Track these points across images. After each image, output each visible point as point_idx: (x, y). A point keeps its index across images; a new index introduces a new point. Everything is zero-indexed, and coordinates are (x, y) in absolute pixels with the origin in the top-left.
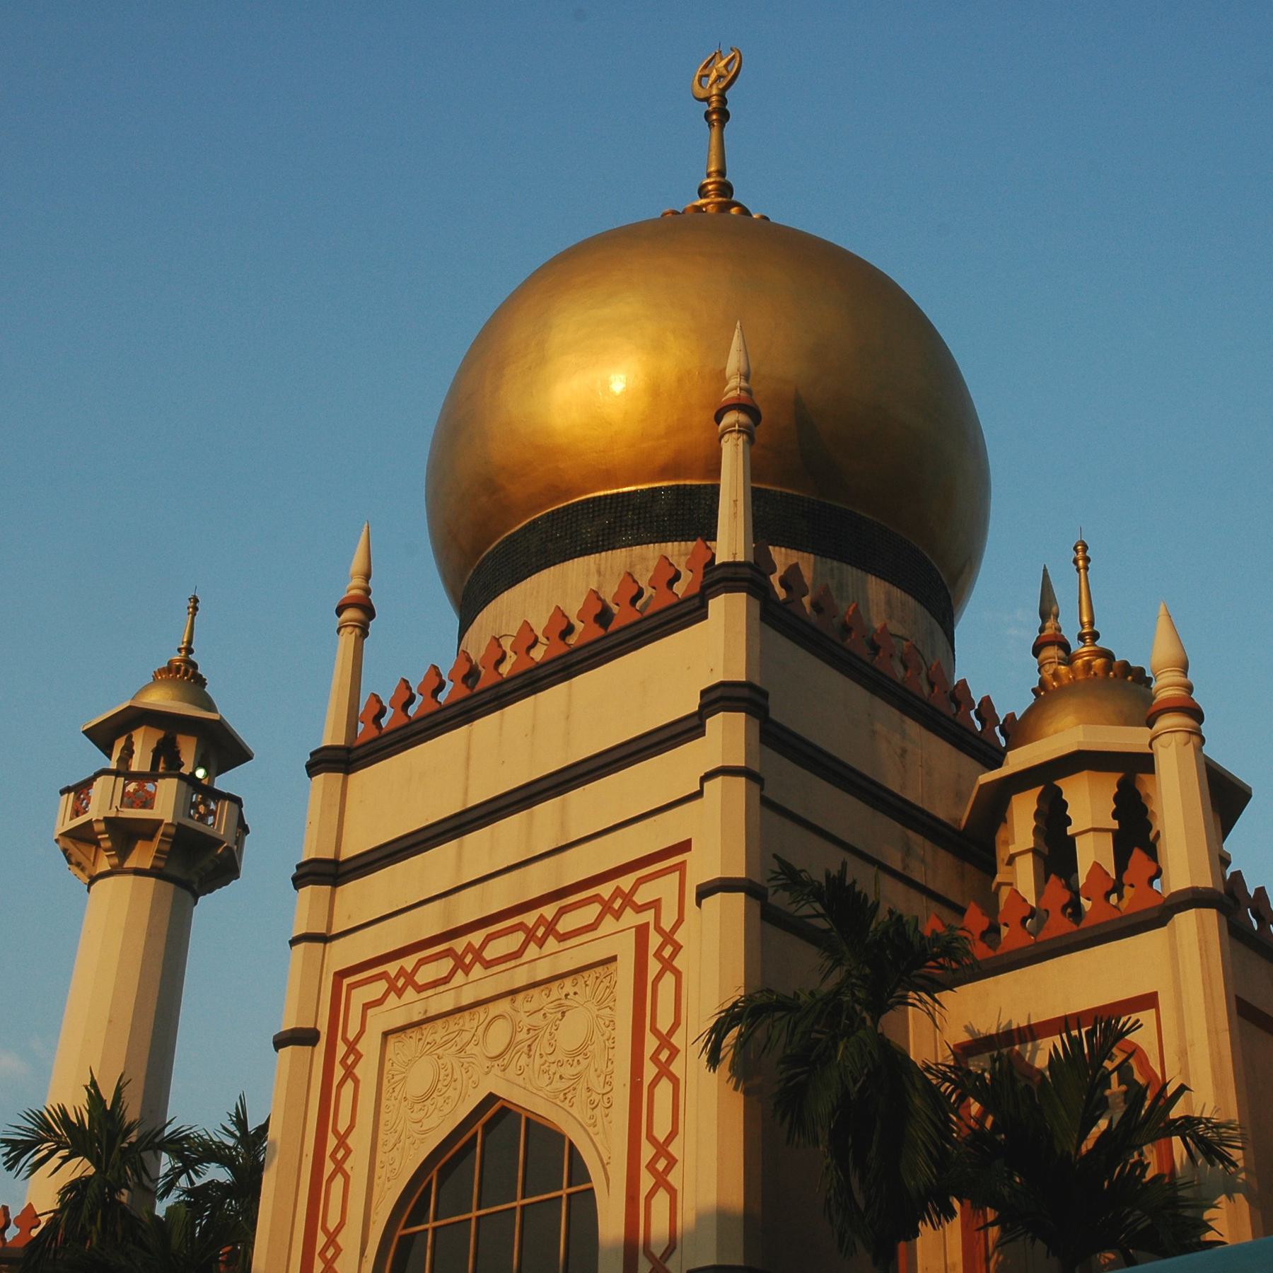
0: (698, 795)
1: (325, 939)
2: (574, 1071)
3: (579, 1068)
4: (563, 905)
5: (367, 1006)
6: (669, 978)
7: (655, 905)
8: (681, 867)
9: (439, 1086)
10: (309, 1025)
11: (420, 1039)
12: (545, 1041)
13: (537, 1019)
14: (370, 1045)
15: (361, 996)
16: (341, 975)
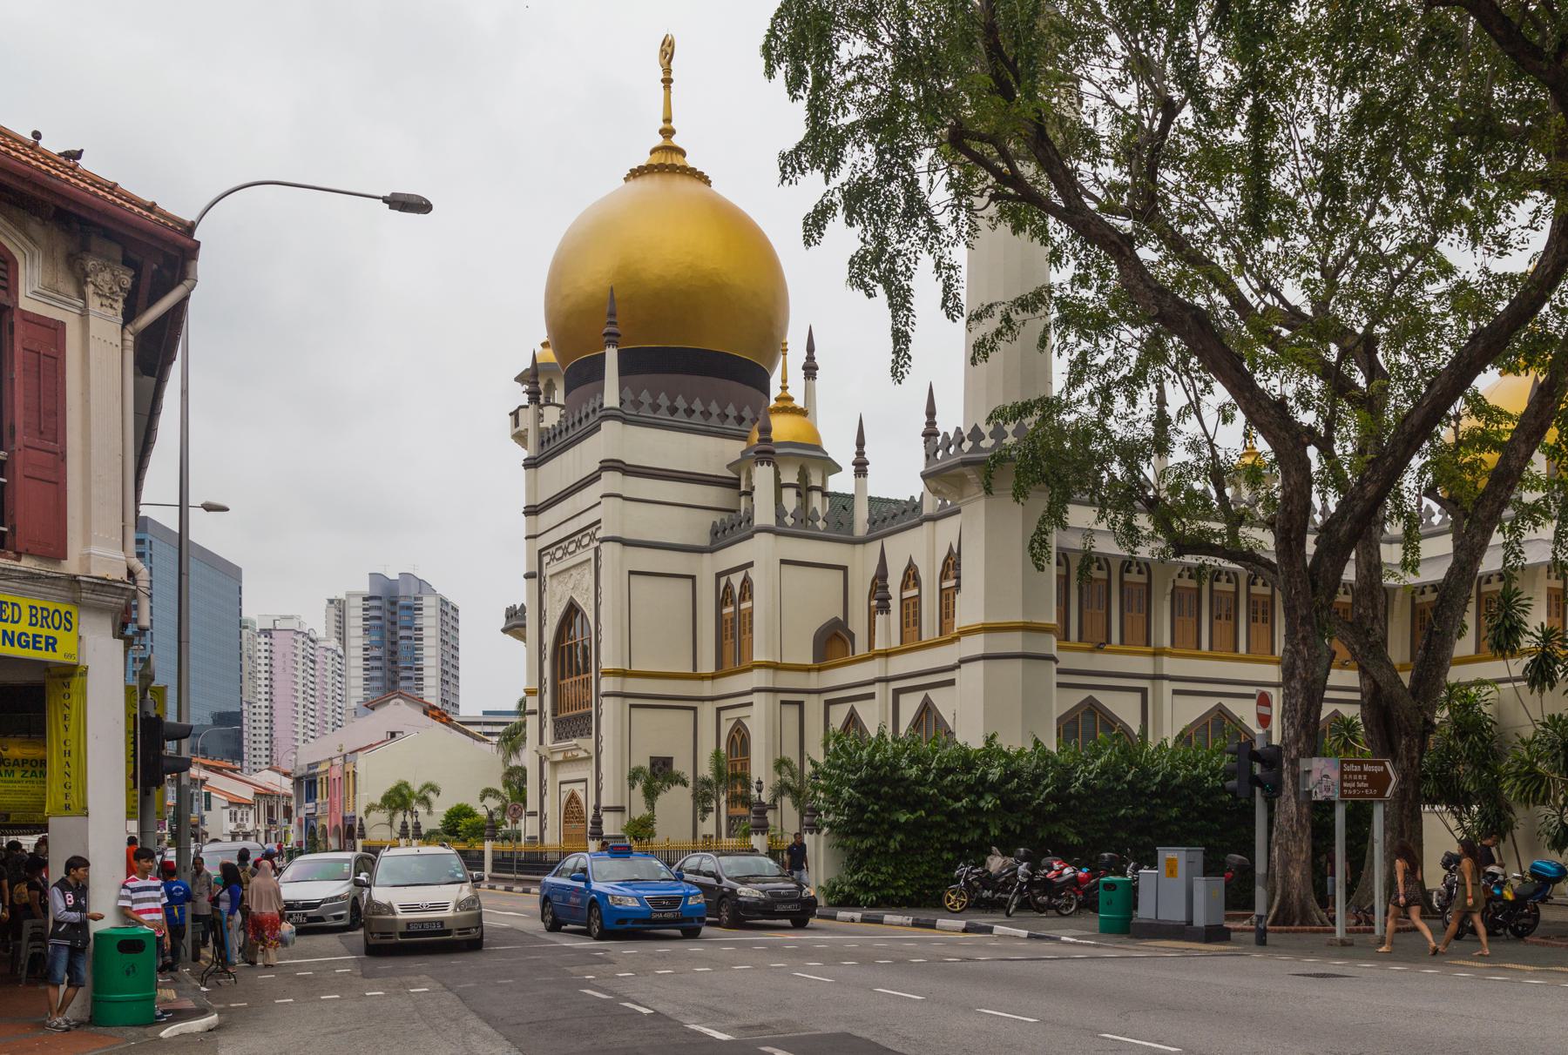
1: (535, 537)
14: (548, 579)
15: (546, 559)
16: (540, 551)
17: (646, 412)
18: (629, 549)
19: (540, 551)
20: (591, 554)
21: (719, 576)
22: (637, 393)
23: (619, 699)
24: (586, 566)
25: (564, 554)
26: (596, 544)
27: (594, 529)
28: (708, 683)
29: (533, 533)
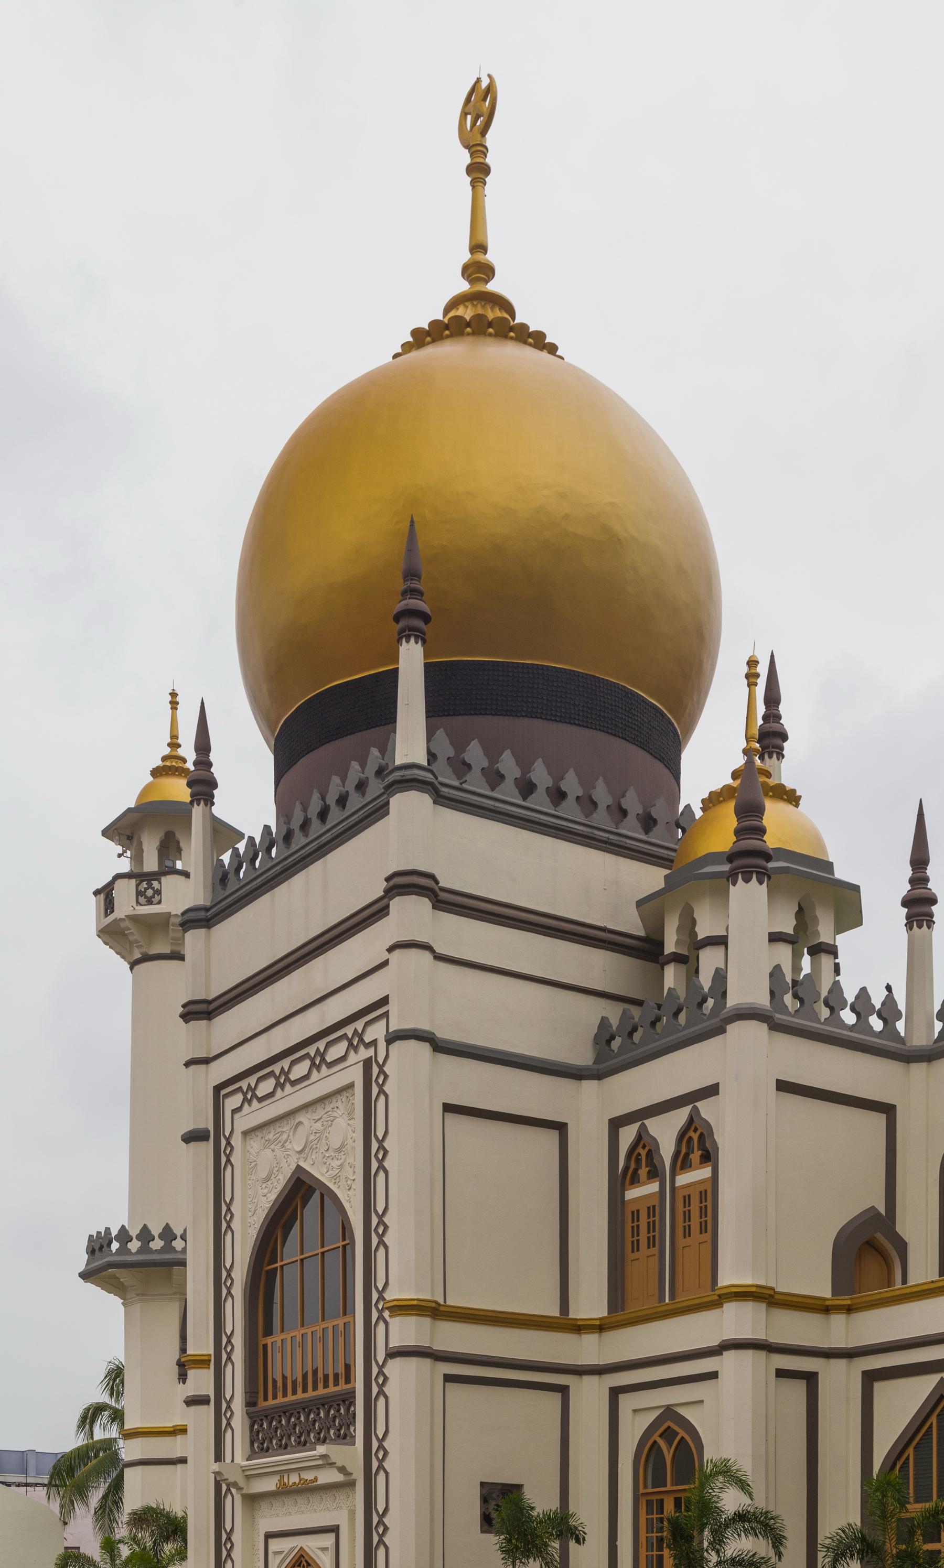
0: (385, 963)
1: (206, 1061)
2: (339, 1163)
3: (342, 1161)
4: (329, 1040)
5: (234, 1111)
6: (382, 1098)
7: (374, 1043)
8: (386, 1014)
9: (274, 1172)
10: (201, 1126)
11: (262, 1138)
12: (324, 1141)
13: (318, 1125)
14: (236, 1141)
15: (234, 1101)
17: (476, 783)
18: (444, 1059)
19: (218, 1089)
20: (355, 1074)
21: (616, 1124)
22: (460, 745)
23: (427, 1362)
24: (340, 1104)
25: (280, 1085)
26: (365, 1053)
27: (359, 1025)
28: (590, 1340)
29: (202, 1054)
